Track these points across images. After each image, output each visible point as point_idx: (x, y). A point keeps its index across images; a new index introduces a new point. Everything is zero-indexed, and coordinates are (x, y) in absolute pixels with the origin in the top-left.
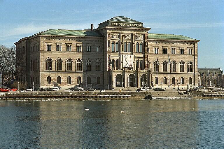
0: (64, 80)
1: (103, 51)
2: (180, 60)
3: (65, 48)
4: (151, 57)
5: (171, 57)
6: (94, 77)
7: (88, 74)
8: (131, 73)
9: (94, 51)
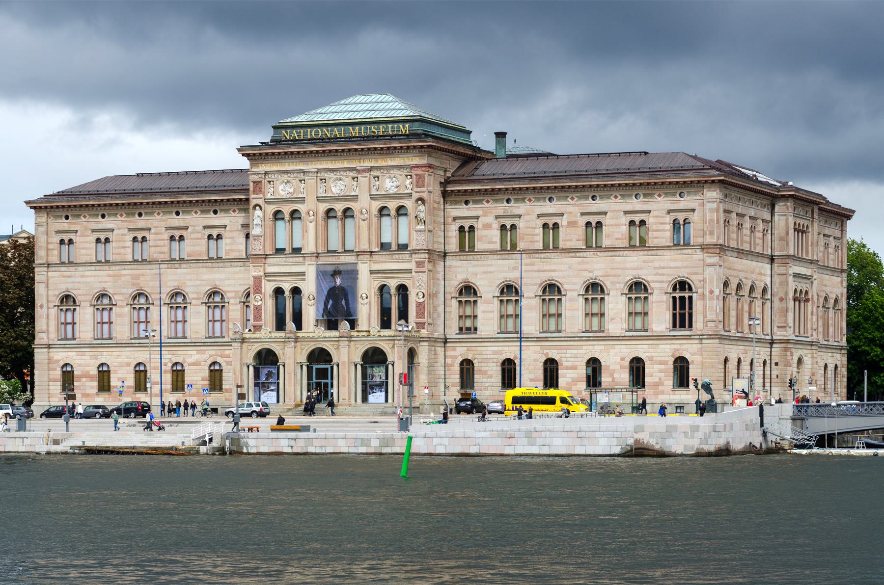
0: (120, 376)
2: (629, 276)
3: (122, 251)
5: (583, 263)
7: (214, 352)
8: (312, 346)
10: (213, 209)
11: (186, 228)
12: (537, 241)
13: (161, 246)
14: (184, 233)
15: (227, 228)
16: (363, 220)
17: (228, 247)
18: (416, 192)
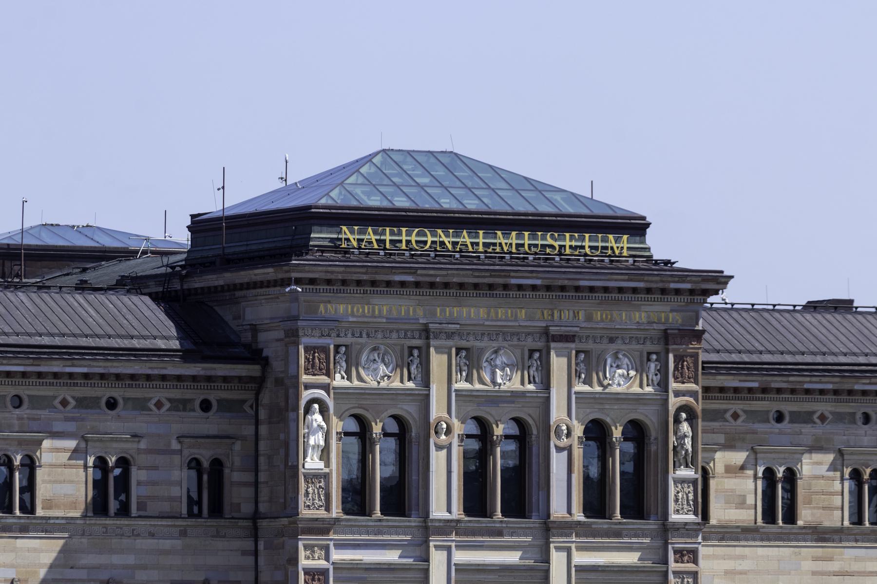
1: (247, 508)
4: (729, 565)
9: (166, 507)
10: (108, 395)
12: (836, 508)
15: (143, 445)
16: (559, 449)
17: (144, 491)
18: (677, 394)
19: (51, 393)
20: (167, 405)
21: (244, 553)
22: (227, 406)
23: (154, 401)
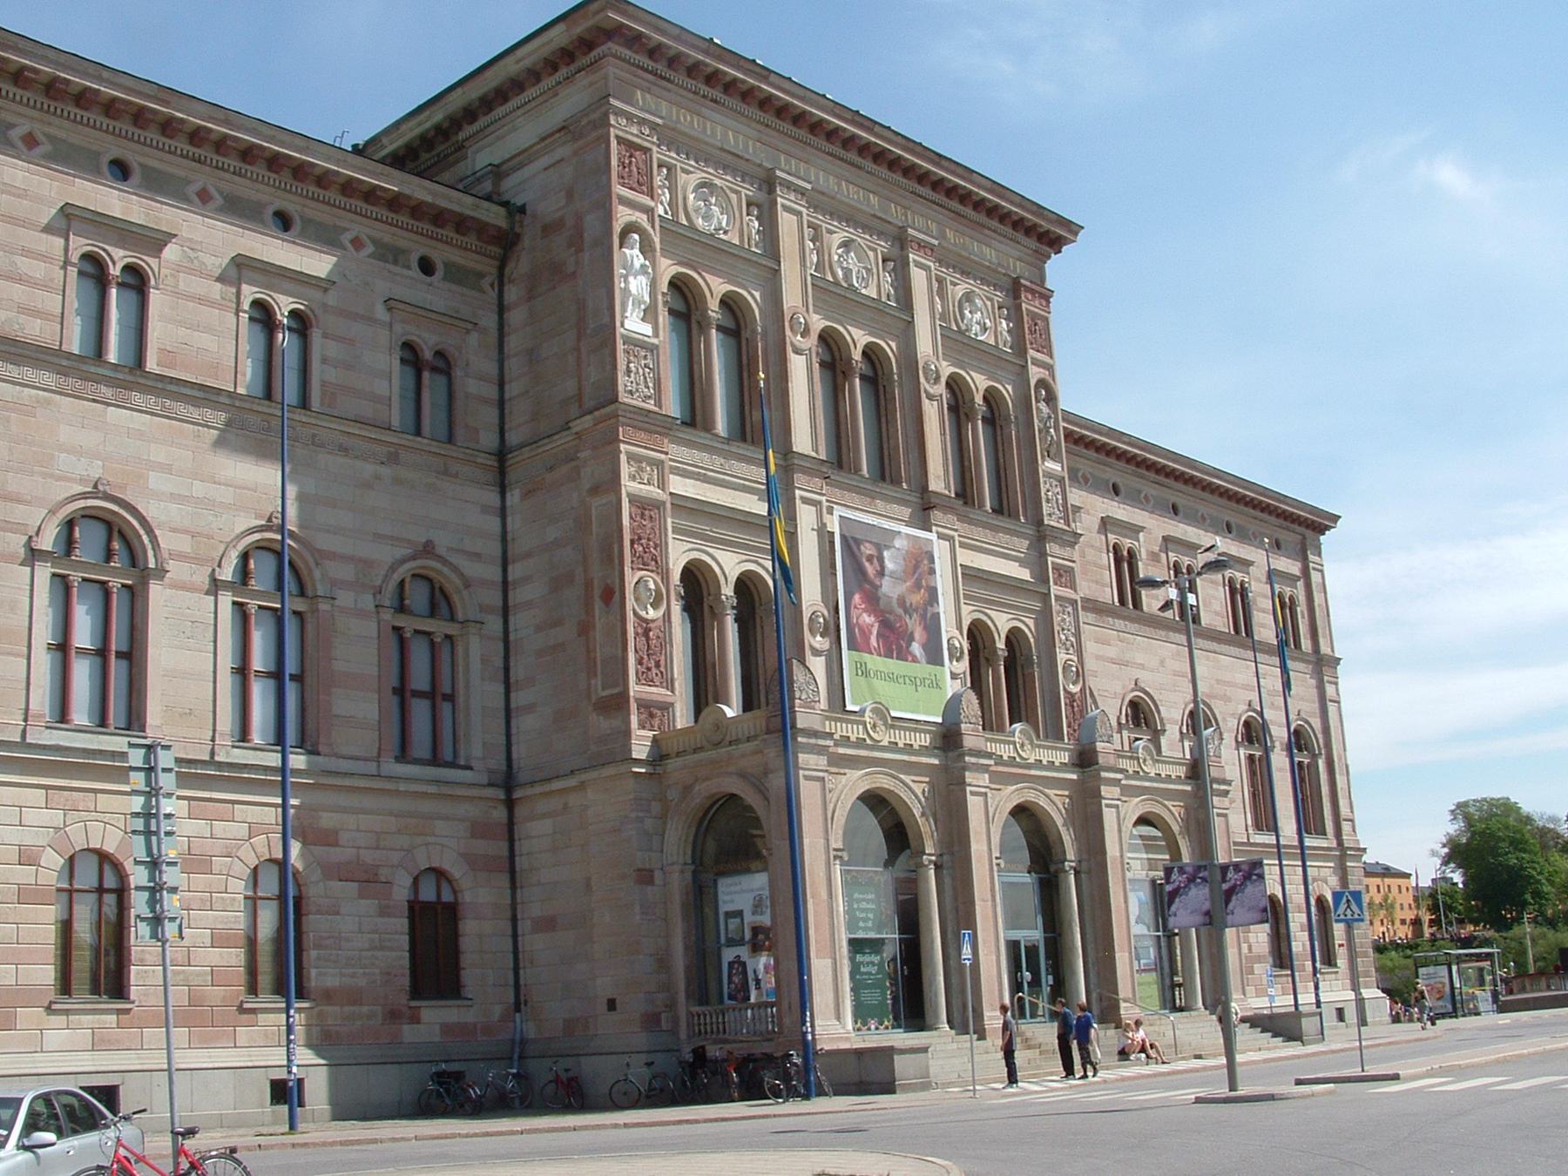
1: (489, 440)
6: (368, 879)
11: (155, 241)
13: (34, 284)
14: (149, 263)
17: (332, 375)
19: (182, 173)
20: (370, 249)
21: (485, 509)
22: (457, 275)
23: (349, 236)
